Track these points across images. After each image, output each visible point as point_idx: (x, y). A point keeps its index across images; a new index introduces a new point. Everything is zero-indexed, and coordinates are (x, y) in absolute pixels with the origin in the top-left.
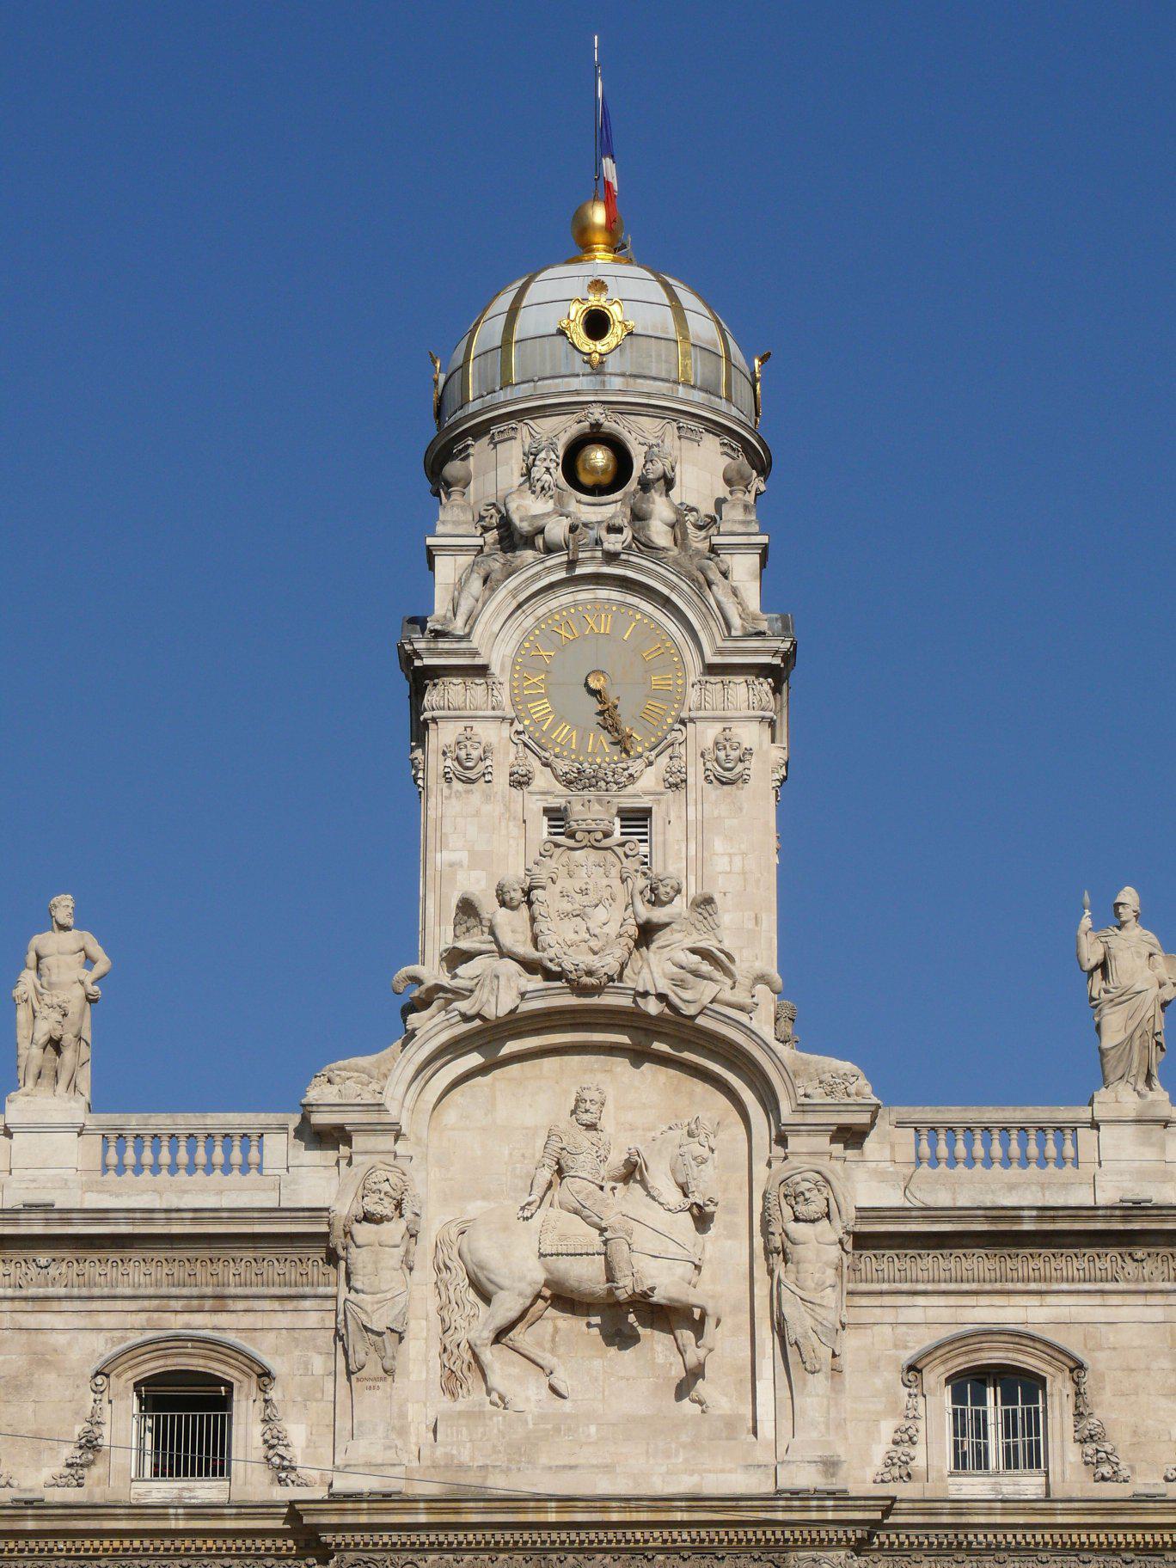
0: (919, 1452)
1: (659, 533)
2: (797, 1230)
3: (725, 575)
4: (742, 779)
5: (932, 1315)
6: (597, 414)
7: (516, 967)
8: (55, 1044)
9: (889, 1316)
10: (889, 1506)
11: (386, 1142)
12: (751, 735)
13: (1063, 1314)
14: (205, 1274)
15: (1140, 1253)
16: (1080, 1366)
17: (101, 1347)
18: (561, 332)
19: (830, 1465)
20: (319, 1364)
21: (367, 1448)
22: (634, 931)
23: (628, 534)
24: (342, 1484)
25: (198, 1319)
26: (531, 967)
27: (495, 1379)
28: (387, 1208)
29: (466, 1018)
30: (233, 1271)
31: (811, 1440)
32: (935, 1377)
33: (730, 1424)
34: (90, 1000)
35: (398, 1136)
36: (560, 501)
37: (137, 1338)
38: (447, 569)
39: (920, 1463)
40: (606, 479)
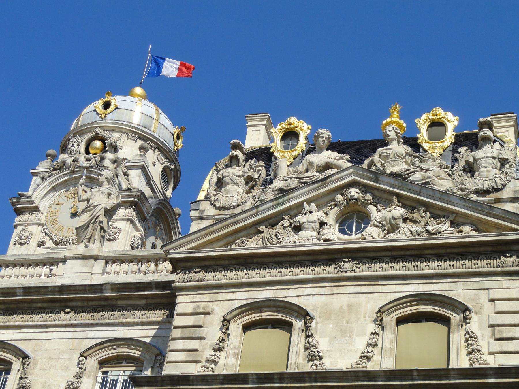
4: (116, 239)
6: (98, 130)
15: (67, 310)
16: (25, 357)
38: (36, 180)
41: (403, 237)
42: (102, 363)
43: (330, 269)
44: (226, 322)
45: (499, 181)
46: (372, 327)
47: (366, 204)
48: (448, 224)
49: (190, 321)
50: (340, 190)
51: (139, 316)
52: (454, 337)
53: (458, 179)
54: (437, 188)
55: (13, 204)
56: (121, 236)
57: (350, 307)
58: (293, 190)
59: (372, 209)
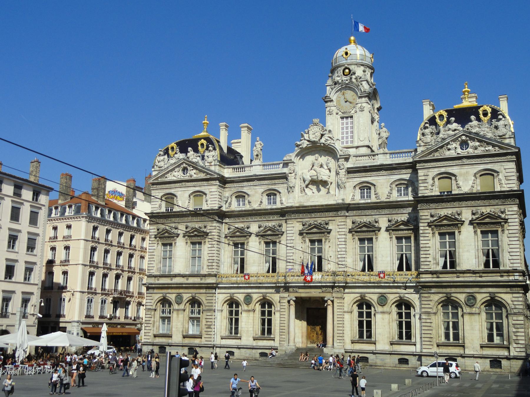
0: (355, 197)
1: (354, 80)
2: (340, 171)
3: (361, 84)
4: (364, 110)
5: (357, 180)
6: (346, 66)
7: (306, 141)
8: (257, 155)
9: (352, 180)
10: (349, 204)
11: (293, 164)
12: (364, 105)
13: (373, 179)
14: (274, 182)
16: (374, 185)
17: (263, 190)
18: (342, 56)
19: (343, 200)
20: (286, 191)
21: (291, 201)
22: (320, 135)
23: (349, 81)
24: (288, 205)
25: (273, 186)
26: (308, 141)
27: (306, 191)
28: (292, 172)
29: (301, 148)
30: (276, 181)
31: (342, 197)
32: (357, 188)
33: (332, 195)
34: (261, 150)
35: (294, 163)
36: (342, 78)
37: (266, 189)
38: (328, 88)
39: (355, 198)
40: (348, 74)
41: (479, 152)
42: (396, 185)
43: (460, 161)
44: (433, 179)
45: (505, 133)
46: (473, 178)
47: (467, 140)
48: (491, 147)
49: (423, 178)
50: (460, 137)
51: (404, 171)
52: (495, 180)
53: (493, 131)
54: (487, 137)
55: (323, 99)
56: (365, 109)
57: (467, 172)
58: (446, 138)
59: (469, 142)
